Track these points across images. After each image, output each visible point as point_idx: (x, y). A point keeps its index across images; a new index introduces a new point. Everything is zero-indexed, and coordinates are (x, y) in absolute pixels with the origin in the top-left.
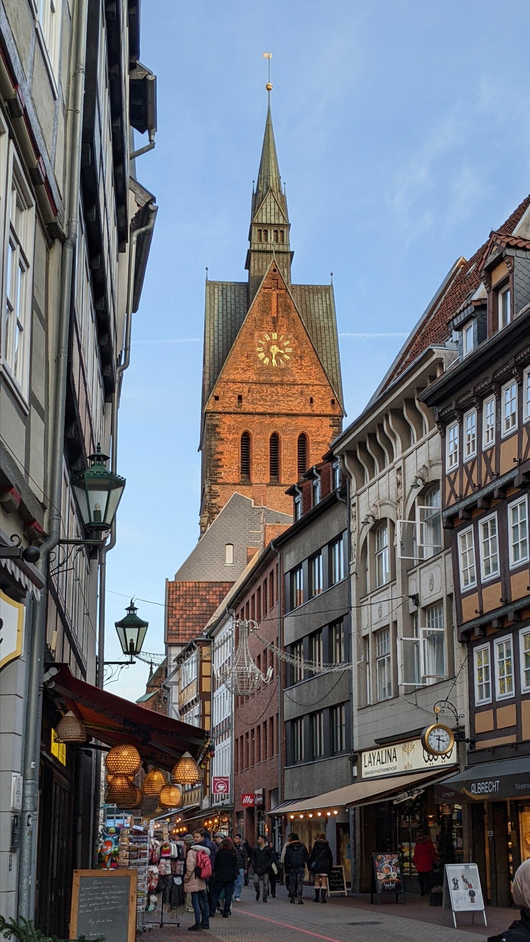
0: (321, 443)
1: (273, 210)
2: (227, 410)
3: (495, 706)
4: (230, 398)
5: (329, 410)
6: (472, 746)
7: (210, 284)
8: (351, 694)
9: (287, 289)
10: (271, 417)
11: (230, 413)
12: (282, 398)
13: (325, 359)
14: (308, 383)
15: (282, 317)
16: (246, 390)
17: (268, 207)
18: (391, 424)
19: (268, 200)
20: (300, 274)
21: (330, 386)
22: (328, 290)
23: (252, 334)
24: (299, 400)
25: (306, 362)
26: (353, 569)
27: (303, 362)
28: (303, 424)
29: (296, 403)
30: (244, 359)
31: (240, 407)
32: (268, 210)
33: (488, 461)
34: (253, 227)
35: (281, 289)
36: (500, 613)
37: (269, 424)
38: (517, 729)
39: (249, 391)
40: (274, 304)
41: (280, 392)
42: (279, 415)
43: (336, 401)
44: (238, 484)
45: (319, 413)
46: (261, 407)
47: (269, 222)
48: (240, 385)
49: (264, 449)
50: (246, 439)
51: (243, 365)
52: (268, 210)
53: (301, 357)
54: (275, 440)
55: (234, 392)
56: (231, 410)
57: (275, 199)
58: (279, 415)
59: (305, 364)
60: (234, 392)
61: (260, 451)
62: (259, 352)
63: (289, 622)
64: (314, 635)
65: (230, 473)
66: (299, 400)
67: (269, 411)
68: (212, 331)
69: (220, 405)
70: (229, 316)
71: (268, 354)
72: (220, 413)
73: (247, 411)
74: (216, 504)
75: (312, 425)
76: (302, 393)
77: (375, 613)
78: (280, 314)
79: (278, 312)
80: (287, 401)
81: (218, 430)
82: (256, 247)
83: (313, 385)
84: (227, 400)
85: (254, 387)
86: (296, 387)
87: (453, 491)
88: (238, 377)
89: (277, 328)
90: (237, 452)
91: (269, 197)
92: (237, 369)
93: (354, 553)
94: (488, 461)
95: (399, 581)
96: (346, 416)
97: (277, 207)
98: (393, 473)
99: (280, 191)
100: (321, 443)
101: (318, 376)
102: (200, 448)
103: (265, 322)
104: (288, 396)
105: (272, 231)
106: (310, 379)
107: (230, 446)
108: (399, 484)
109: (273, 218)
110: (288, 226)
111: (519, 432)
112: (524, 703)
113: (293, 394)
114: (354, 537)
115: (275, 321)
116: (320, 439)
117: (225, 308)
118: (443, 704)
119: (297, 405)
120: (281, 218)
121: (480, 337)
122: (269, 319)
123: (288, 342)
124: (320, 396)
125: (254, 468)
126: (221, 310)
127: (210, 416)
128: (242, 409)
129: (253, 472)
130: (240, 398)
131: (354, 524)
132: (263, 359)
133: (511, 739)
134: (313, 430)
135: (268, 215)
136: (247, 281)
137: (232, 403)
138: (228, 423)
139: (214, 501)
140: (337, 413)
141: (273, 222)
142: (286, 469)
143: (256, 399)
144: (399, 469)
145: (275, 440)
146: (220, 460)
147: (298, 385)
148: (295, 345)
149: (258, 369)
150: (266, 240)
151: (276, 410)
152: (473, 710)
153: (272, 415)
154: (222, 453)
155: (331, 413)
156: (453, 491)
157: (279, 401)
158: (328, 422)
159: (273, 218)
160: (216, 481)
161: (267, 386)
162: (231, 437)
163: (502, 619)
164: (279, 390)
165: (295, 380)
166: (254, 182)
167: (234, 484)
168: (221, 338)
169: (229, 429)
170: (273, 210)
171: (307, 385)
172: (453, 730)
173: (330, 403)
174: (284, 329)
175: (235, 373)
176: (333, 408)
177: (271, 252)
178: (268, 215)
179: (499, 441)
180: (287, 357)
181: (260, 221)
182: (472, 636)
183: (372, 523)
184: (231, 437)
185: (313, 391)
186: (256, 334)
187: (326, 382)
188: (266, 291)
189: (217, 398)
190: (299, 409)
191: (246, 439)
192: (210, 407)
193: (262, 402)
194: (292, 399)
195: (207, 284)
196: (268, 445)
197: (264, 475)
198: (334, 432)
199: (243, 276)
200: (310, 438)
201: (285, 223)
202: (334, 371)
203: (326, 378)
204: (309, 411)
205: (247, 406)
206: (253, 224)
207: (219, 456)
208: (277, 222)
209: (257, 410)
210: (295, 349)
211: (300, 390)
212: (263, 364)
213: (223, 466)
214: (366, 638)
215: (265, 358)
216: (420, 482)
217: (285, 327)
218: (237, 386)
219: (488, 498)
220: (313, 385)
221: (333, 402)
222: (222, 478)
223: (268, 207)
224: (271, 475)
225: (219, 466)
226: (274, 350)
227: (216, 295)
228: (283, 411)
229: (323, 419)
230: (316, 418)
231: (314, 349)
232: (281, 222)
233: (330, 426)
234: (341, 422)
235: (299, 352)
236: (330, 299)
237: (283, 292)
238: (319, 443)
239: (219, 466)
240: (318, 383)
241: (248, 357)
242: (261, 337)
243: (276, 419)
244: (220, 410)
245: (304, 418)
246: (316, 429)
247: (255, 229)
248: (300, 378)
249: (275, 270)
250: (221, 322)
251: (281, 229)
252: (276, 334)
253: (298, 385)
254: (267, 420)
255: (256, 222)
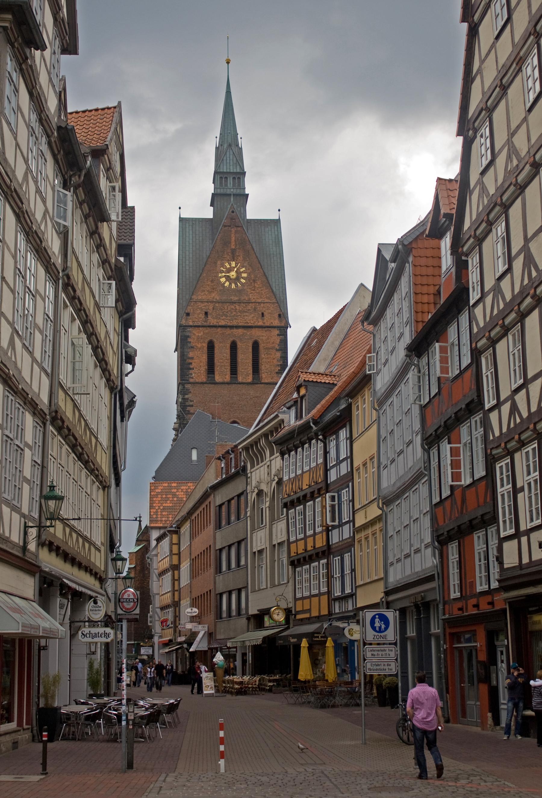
0: (271, 348)
1: (231, 161)
2: (196, 324)
3: (303, 598)
4: (199, 314)
5: (276, 323)
6: (295, 617)
7: (181, 220)
8: (248, 583)
9: (242, 227)
10: (231, 329)
11: (199, 326)
12: (239, 314)
13: (273, 280)
14: (260, 301)
15: (239, 249)
16: (211, 308)
17: (228, 159)
18: (263, 442)
19: (228, 153)
20: (254, 211)
21: (278, 303)
22: (277, 222)
23: (215, 263)
24: (253, 315)
25: (258, 284)
26: (248, 514)
27: (256, 284)
28: (257, 334)
29: (250, 318)
30: (209, 283)
31: (206, 321)
32: (228, 161)
33: (299, 480)
34: (216, 175)
35: (238, 227)
36: (303, 555)
37: (229, 334)
38: (309, 611)
39: (213, 309)
40: (233, 239)
41: (238, 309)
42: (237, 327)
43: (282, 315)
44: (206, 383)
45: (268, 325)
46: (222, 321)
47: (228, 171)
48: (206, 304)
49: (225, 355)
50: (211, 347)
51: (208, 288)
52: (228, 161)
53: (254, 281)
54: (234, 347)
55: (201, 309)
56: (200, 324)
57: (233, 153)
58: (237, 327)
59: (257, 286)
60: (201, 309)
61: (222, 355)
62: (221, 277)
63: (218, 534)
64: (230, 546)
65: (199, 374)
66: (253, 315)
67: (229, 324)
68: (184, 259)
69: (191, 320)
70: (198, 247)
71: (228, 278)
72: (191, 326)
73: (212, 324)
74: (188, 399)
75: (263, 334)
76: (255, 309)
77: (259, 540)
78: (238, 247)
79: (236, 245)
80: (244, 316)
81: (189, 340)
82: (219, 191)
83: (264, 303)
84: (196, 316)
85: (217, 305)
86: (251, 304)
87: (286, 490)
88: (204, 297)
89: (235, 258)
90: (205, 357)
91: (228, 151)
92: (204, 291)
93: (249, 505)
94: (299, 480)
95: (268, 526)
96: (290, 327)
97: (235, 159)
98: (266, 466)
99: (238, 145)
100: (271, 348)
101: (268, 295)
102: (176, 350)
103: (225, 253)
104: (244, 312)
105: (231, 179)
106: (261, 298)
107: (199, 353)
108: (268, 474)
109: (231, 167)
110: (244, 173)
111: (309, 470)
112: (313, 599)
113: (249, 310)
114: (249, 497)
115: (233, 252)
116: (270, 346)
117: (194, 240)
118: (280, 597)
119: (251, 319)
120: (238, 167)
121: (296, 418)
122: (229, 251)
123: (244, 269)
124: (270, 311)
125: (217, 369)
126: (191, 242)
127: (183, 329)
128: (208, 323)
129: (216, 373)
130: (206, 313)
131: (249, 488)
132: (224, 283)
133: (307, 615)
134: (264, 338)
135: (228, 165)
136: (212, 217)
137: (200, 318)
138: (197, 335)
139: (186, 396)
140: (283, 325)
141: (232, 171)
142: (243, 370)
143: (219, 315)
144: (268, 466)
145: (234, 347)
146: (191, 363)
147: (252, 303)
148: (249, 271)
149: (220, 290)
150: (226, 185)
151: (235, 323)
152: (296, 599)
153: (231, 327)
154: (192, 358)
155: (279, 325)
156: (286, 490)
157: (237, 316)
158: (276, 332)
159: (231, 167)
160: (188, 380)
161: (228, 304)
162: (199, 346)
163: (304, 558)
164: (237, 307)
165: (249, 299)
166: (216, 137)
167: (202, 383)
168: (191, 264)
169: (198, 338)
170: (231, 161)
171: (259, 303)
172: (285, 609)
173: (277, 317)
174: (241, 258)
175: (202, 294)
176: (281, 321)
177: (230, 195)
178: (228, 165)
179: (303, 472)
180: (243, 281)
181: (222, 170)
182: (296, 563)
183: (256, 491)
184: (199, 346)
185: (264, 307)
186: (219, 263)
187: (274, 301)
188: (226, 228)
189: (188, 314)
190: (252, 322)
191: (211, 347)
192: (183, 322)
193: (224, 317)
194: (246, 314)
195: (180, 221)
196: (228, 351)
197: (226, 375)
198: (280, 340)
199: (208, 213)
200: (261, 346)
201: (241, 171)
202: (281, 290)
203: (274, 297)
204: (260, 324)
205: (212, 321)
206: (216, 173)
207: (190, 361)
208: (235, 171)
209: (220, 324)
210: (249, 274)
211: (253, 307)
212: (224, 287)
213: (193, 369)
214: (255, 553)
215: (226, 281)
216: (276, 478)
217: (241, 257)
218: (204, 305)
219: (298, 499)
220: (264, 303)
221: (280, 316)
222: (192, 378)
223: (228, 159)
224: (231, 374)
225: (190, 369)
226: (233, 274)
227: (188, 230)
228: (240, 324)
229: (272, 330)
230: (266, 329)
231: (264, 274)
232: (238, 171)
233: (278, 335)
234: (287, 332)
235: (253, 276)
236: (277, 230)
237: (239, 229)
238: (268, 349)
239: (190, 369)
240: (267, 301)
241: (212, 281)
242: (223, 265)
243: (235, 330)
244: (191, 324)
245: (257, 329)
246: (267, 337)
247: (218, 177)
248: (253, 297)
249: (233, 212)
250: (191, 252)
251: (238, 176)
252: (234, 263)
253: (252, 303)
254: (228, 331)
255: (219, 171)
